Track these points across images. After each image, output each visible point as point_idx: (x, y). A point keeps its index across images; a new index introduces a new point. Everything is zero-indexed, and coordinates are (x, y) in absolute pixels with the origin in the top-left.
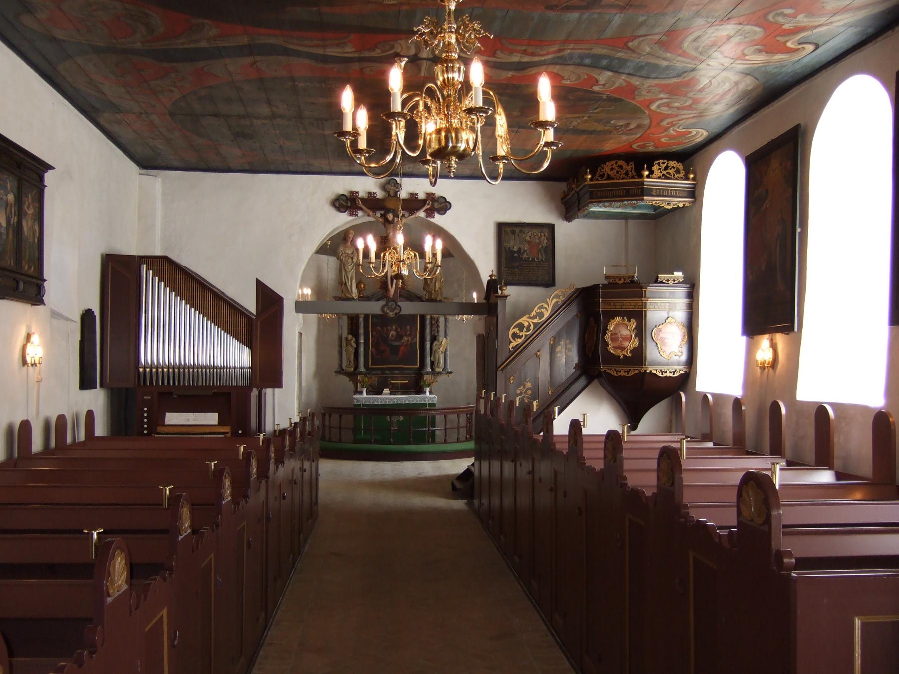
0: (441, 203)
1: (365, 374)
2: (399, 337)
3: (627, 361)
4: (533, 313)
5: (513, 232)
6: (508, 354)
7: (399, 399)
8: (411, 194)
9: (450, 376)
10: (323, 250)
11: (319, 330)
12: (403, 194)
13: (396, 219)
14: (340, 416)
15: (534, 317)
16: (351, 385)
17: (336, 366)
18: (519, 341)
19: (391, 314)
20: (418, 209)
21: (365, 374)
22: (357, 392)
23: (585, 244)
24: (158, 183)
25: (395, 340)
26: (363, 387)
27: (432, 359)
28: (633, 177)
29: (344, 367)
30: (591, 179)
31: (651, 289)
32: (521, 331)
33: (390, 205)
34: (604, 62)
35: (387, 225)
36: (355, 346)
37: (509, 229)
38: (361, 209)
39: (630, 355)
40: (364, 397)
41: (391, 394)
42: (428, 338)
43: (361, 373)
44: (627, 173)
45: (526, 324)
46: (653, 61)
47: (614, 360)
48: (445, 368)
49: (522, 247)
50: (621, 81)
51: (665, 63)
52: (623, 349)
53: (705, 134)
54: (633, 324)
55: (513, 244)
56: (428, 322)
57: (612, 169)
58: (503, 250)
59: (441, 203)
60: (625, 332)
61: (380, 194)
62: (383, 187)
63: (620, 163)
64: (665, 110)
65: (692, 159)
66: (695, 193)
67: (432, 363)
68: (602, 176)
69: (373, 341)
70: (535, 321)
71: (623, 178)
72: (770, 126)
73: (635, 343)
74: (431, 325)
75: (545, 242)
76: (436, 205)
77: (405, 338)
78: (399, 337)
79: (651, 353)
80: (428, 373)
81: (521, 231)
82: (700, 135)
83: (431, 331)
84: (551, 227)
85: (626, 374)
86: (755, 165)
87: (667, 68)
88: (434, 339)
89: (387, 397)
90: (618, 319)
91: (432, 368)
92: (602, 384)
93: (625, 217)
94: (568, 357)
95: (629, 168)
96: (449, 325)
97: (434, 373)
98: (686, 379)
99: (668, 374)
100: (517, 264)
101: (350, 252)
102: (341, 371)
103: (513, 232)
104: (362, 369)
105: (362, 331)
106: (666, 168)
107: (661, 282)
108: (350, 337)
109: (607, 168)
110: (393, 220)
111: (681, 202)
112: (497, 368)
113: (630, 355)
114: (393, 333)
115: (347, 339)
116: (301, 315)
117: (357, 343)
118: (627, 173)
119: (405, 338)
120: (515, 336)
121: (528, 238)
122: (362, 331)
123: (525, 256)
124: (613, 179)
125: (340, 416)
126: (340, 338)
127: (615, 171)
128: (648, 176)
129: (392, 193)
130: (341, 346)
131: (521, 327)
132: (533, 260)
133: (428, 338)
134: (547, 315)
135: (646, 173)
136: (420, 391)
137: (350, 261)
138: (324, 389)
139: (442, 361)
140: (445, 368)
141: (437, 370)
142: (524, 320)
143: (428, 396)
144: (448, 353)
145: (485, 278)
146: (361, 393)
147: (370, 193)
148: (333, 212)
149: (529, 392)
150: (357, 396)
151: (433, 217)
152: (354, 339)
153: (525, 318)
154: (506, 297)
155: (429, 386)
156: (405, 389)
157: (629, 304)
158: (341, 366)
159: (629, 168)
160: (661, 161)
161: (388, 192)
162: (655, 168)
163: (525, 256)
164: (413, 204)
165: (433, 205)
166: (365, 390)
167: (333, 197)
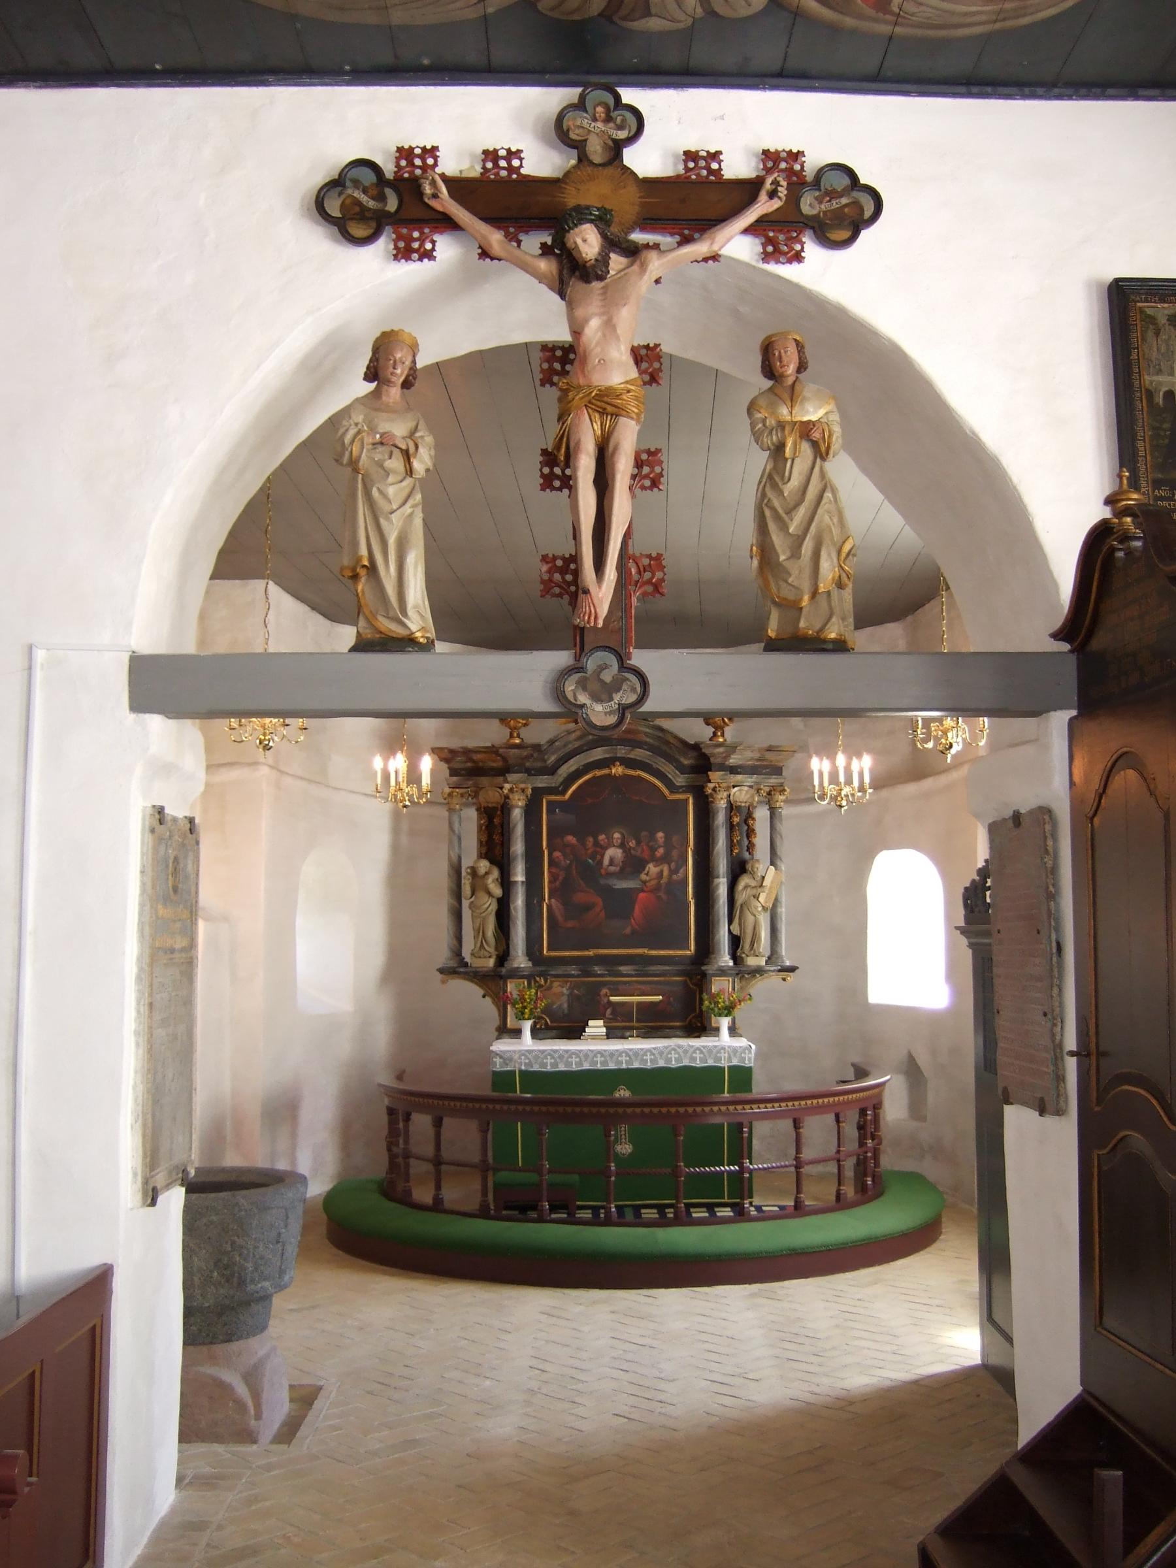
0: (832, 194)
1: (530, 978)
7: (636, 1053)
8: (690, 156)
9: (791, 978)
11: (395, 848)
12: (648, 159)
13: (617, 261)
16: (488, 1007)
17: (442, 955)
21: (530, 978)
22: (506, 1031)
25: (622, 874)
26: (521, 1016)
27: (736, 932)
35: (576, 287)
36: (498, 892)
38: (447, 223)
40: (525, 1049)
41: (609, 1036)
42: (722, 865)
43: (515, 974)
48: (773, 957)
56: (721, 818)
58: (1141, 405)
59: (832, 194)
61: (541, 161)
62: (561, 131)
67: (735, 942)
74: (731, 827)
76: (809, 205)
77: (652, 869)
80: (723, 972)
83: (731, 845)
88: (739, 869)
89: (596, 1048)
96: (784, 827)
97: (742, 972)
102: (457, 968)
104: (520, 959)
105: (518, 847)
108: (484, 865)
110: (603, 260)
115: (474, 872)
116: (155, 722)
117: (506, 882)
119: (652, 869)
122: (518, 847)
126: (456, 870)
129: (596, 150)
130: (457, 894)
133: (722, 865)
136: (699, 1026)
137: (396, 464)
138: (410, 1026)
140: (773, 957)
141: (752, 962)
143: (725, 1045)
144: (782, 910)
146: (517, 1033)
147: (491, 155)
148: (318, 242)
150: (503, 1046)
151: (798, 258)
152: (496, 873)
155: (729, 1010)
156: (653, 1023)
158: (457, 953)
161: (579, 146)
164: (696, 200)
165: (794, 199)
166: (527, 1026)
167: (319, 178)
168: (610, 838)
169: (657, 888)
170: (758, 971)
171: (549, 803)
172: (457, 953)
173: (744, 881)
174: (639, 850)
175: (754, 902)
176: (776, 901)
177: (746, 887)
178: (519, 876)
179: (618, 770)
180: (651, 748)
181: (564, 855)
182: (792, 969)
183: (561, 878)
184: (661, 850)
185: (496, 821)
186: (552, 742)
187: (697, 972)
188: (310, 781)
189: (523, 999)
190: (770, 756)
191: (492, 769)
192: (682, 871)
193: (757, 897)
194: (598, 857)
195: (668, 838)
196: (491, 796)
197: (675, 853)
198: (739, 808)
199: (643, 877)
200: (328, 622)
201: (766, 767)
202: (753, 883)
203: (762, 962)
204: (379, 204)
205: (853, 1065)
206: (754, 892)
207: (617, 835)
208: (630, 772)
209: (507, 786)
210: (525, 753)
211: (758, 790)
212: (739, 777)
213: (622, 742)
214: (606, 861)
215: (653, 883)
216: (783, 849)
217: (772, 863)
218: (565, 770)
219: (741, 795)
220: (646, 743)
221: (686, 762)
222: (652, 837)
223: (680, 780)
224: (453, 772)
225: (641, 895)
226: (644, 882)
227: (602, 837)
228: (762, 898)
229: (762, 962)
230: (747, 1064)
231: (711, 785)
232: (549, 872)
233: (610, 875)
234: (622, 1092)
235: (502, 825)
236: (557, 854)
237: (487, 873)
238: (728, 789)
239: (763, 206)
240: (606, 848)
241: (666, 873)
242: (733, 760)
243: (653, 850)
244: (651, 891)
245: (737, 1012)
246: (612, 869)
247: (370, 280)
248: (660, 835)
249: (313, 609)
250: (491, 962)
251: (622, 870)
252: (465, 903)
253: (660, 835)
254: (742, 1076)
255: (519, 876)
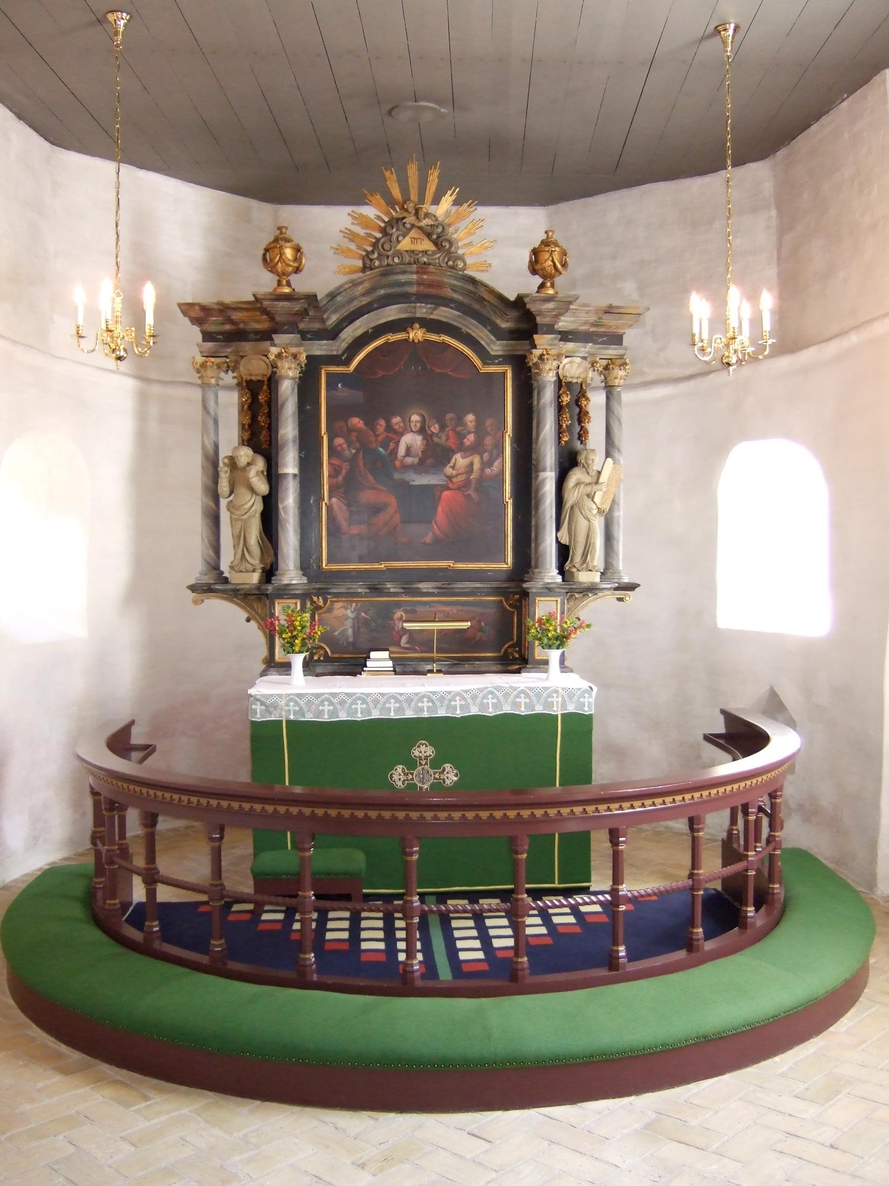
1: (305, 597)
2: (436, 456)
11: (142, 438)
16: (254, 633)
17: (194, 569)
21: (305, 597)
22: (275, 665)
25: (421, 466)
26: (290, 648)
27: (565, 540)
29: (224, 567)
36: (263, 487)
40: (296, 692)
43: (285, 592)
56: (548, 395)
67: (564, 552)
69: (335, 472)
77: (460, 461)
78: (436, 456)
80: (549, 590)
88: (569, 461)
91: (561, 571)
97: (573, 591)
102: (214, 584)
104: (291, 573)
105: (288, 430)
108: (245, 454)
114: (411, 440)
115: (233, 463)
117: (273, 476)
126: (212, 462)
136: (515, 657)
138: (159, 656)
141: (584, 577)
144: (620, 514)
146: (286, 667)
150: (268, 688)
152: (260, 464)
156: (460, 654)
166: (298, 661)
168: (406, 421)
169: (466, 484)
170: (592, 589)
171: (328, 375)
172: (215, 567)
173: (575, 476)
174: (444, 438)
175: (588, 503)
177: (578, 484)
178: (290, 465)
179: (417, 334)
180: (460, 307)
181: (350, 444)
182: (632, 587)
183: (344, 471)
184: (471, 437)
185: (262, 398)
186: (332, 296)
188: (15, 342)
189: (291, 626)
190: (608, 320)
191: (257, 332)
192: (497, 463)
193: (591, 497)
194: (392, 445)
195: (479, 423)
196: (255, 368)
197: (489, 441)
198: (569, 385)
199: (448, 470)
200: (47, 145)
201: (600, 335)
202: (587, 479)
203: (596, 578)
205: (723, 712)
206: (588, 489)
207: (415, 418)
208: (433, 337)
209: (274, 350)
210: (297, 307)
211: (593, 364)
212: (570, 346)
213: (421, 298)
214: (402, 451)
215: (461, 478)
216: (624, 437)
217: (608, 455)
218: (349, 334)
219: (574, 367)
220: (452, 300)
221: (504, 325)
222: (460, 421)
223: (496, 348)
224: (208, 336)
225: (446, 493)
226: (450, 478)
227: (396, 420)
228: (597, 499)
229: (596, 578)
230: (587, 711)
231: (537, 352)
232: (329, 463)
233: (406, 467)
234: (423, 748)
235: (269, 403)
236: (339, 441)
237: (249, 464)
238: (558, 357)
240: (401, 434)
241: (477, 466)
242: (565, 323)
243: (461, 437)
244: (459, 489)
245: (571, 643)
246: (409, 460)
248: (470, 418)
249: (20, 117)
250: (255, 578)
251: (422, 462)
252: (223, 503)
253: (470, 418)
254: (579, 727)
255: (290, 465)
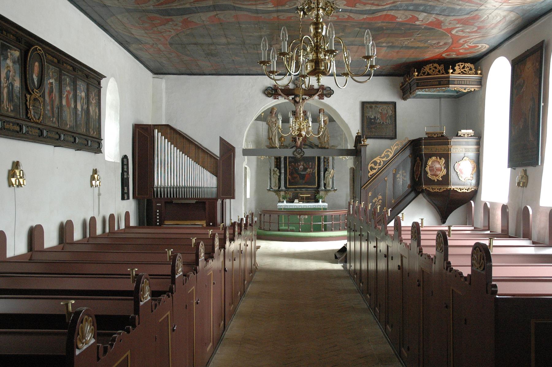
2: (305, 169)
3: (439, 183)
4: (383, 155)
5: (371, 107)
6: (367, 179)
10: (259, 119)
11: (257, 165)
14: (270, 216)
15: (383, 157)
18: (374, 171)
19: (299, 156)
20: (314, 95)
22: (280, 202)
23: (415, 115)
24: (163, 82)
25: (303, 171)
28: (443, 74)
30: (418, 75)
31: (454, 140)
32: (375, 165)
33: (296, 92)
34: (421, 8)
35: (296, 104)
36: (279, 174)
37: (368, 106)
38: (280, 95)
39: (441, 179)
40: (285, 204)
43: (282, 191)
44: (439, 71)
45: (378, 161)
46: (450, 6)
47: (430, 182)
49: (376, 116)
50: (432, 18)
51: (458, 7)
52: (436, 175)
53: (487, 46)
54: (443, 161)
55: (371, 114)
57: (430, 69)
60: (438, 166)
61: (291, 86)
63: (435, 65)
64: (461, 34)
65: (478, 62)
66: (481, 83)
67: (325, 185)
68: (424, 73)
69: (289, 172)
70: (384, 159)
71: (437, 74)
72: (526, 42)
73: (444, 172)
74: (324, 162)
75: (390, 112)
77: (309, 170)
78: (305, 169)
79: (453, 177)
80: (322, 190)
81: (376, 107)
82: (484, 47)
83: (324, 165)
84: (394, 104)
85: (438, 191)
86: (517, 65)
87: (460, 10)
88: (326, 170)
89: (297, 204)
90: (434, 158)
92: (424, 197)
93: (440, 97)
94: (404, 180)
95: (440, 68)
96: (335, 162)
97: (326, 191)
98: (474, 194)
99: (464, 191)
100: (374, 126)
101: (274, 120)
103: (371, 107)
105: (282, 166)
106: (464, 68)
107: (460, 136)
108: (276, 169)
109: (427, 69)
111: (472, 88)
112: (361, 187)
113: (441, 179)
114: (301, 167)
115: (274, 170)
116: (246, 157)
117: (280, 173)
118: (439, 71)
120: (372, 169)
121: (380, 110)
122: (282, 166)
123: (378, 121)
124: (431, 75)
125: (270, 216)
127: (432, 70)
128: (452, 73)
131: (375, 163)
132: (383, 123)
134: (391, 156)
135: (451, 71)
136: (317, 201)
137: (274, 125)
139: (331, 183)
141: (328, 188)
142: (377, 159)
145: (354, 135)
148: (264, 97)
149: (381, 201)
152: (278, 171)
153: (378, 158)
154: (366, 145)
156: (308, 200)
157: (440, 149)
159: (440, 68)
160: (460, 63)
162: (457, 68)
163: (378, 121)
164: (311, 92)
165: (323, 92)
167: (264, 88)
173: (327, 172)
176: (333, 177)
178: (283, 171)
187: (317, 191)
204: (272, 92)
222: (309, 164)
239: (319, 93)
247: (271, 102)
255: (283, 171)
